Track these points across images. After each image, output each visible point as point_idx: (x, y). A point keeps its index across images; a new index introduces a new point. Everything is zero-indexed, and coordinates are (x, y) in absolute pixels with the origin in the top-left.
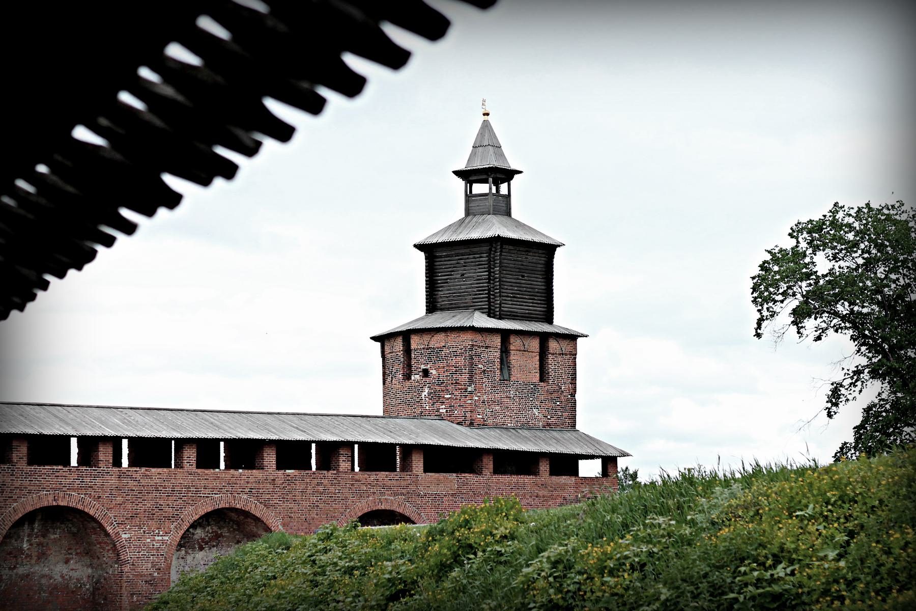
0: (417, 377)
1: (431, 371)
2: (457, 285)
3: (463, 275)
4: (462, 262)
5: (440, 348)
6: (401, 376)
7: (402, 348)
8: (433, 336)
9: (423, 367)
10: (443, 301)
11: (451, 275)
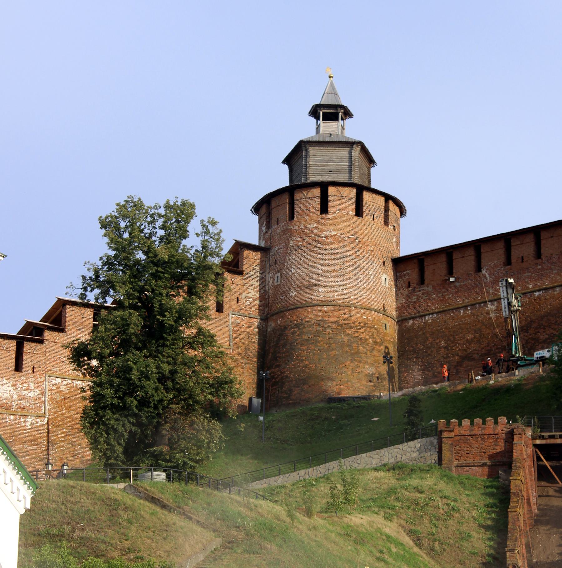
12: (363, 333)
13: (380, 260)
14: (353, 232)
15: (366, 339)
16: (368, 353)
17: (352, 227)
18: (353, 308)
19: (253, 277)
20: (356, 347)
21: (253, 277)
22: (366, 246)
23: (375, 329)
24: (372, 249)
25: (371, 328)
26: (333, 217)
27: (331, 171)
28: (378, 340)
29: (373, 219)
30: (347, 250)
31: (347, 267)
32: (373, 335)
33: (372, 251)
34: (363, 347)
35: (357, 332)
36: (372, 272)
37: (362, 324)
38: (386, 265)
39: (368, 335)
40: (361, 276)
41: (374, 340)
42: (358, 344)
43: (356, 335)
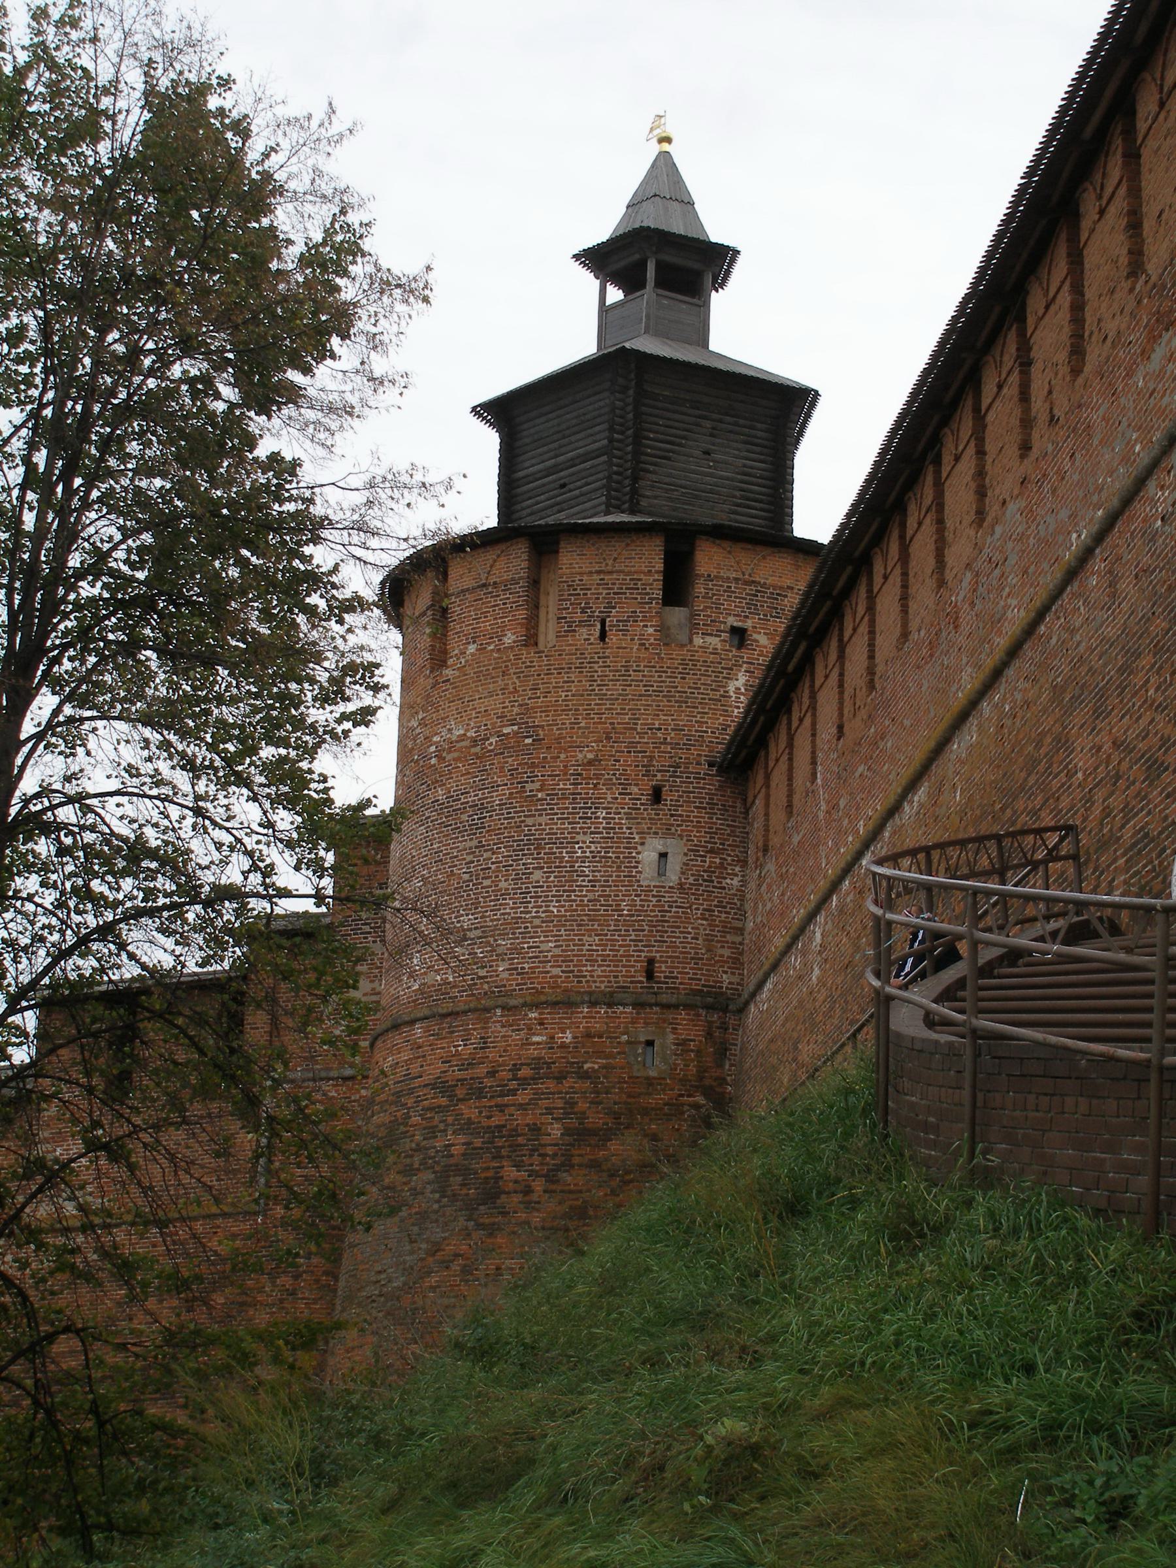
0: (714, 641)
1: (755, 636)
2: (694, 472)
3: (707, 453)
4: (708, 424)
5: (781, 588)
6: (651, 630)
7: (660, 566)
8: (764, 558)
9: (732, 621)
10: (656, 497)
11: (680, 445)
12: (522, 1107)
13: (635, 789)
14: (516, 710)
15: (536, 1130)
16: (538, 1185)
17: (516, 691)
18: (499, 1012)
19: (367, 928)
20: (491, 1174)
21: (367, 928)
22: (561, 750)
23: (585, 1076)
24: (590, 756)
25: (561, 1077)
26: (457, 673)
27: (563, 486)
28: (596, 1119)
29: (603, 636)
30: (494, 787)
31: (486, 855)
32: (572, 1104)
33: (590, 763)
34: (518, 1166)
35: (501, 1108)
36: (586, 845)
37: (524, 1072)
38: (668, 797)
39: (549, 1111)
40: (537, 875)
41: (573, 1122)
42: (497, 1157)
43: (495, 1121)
